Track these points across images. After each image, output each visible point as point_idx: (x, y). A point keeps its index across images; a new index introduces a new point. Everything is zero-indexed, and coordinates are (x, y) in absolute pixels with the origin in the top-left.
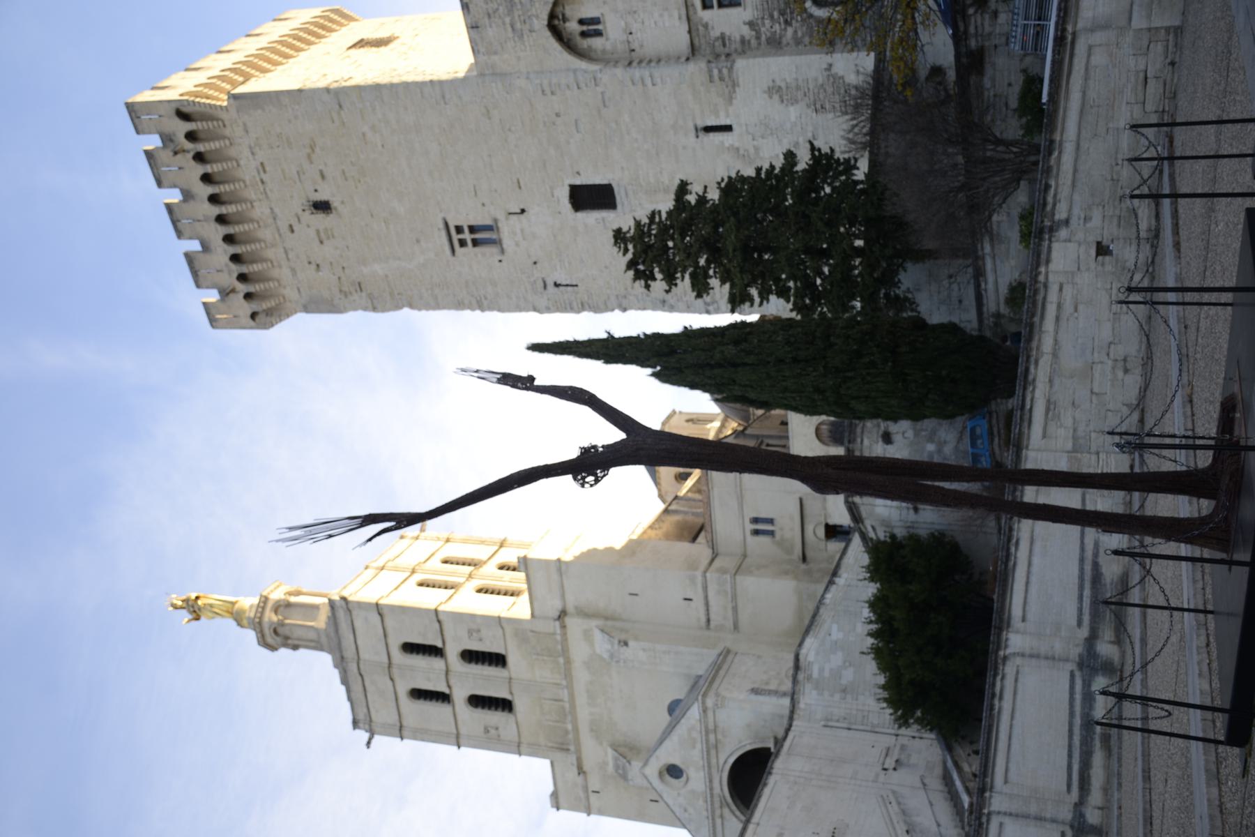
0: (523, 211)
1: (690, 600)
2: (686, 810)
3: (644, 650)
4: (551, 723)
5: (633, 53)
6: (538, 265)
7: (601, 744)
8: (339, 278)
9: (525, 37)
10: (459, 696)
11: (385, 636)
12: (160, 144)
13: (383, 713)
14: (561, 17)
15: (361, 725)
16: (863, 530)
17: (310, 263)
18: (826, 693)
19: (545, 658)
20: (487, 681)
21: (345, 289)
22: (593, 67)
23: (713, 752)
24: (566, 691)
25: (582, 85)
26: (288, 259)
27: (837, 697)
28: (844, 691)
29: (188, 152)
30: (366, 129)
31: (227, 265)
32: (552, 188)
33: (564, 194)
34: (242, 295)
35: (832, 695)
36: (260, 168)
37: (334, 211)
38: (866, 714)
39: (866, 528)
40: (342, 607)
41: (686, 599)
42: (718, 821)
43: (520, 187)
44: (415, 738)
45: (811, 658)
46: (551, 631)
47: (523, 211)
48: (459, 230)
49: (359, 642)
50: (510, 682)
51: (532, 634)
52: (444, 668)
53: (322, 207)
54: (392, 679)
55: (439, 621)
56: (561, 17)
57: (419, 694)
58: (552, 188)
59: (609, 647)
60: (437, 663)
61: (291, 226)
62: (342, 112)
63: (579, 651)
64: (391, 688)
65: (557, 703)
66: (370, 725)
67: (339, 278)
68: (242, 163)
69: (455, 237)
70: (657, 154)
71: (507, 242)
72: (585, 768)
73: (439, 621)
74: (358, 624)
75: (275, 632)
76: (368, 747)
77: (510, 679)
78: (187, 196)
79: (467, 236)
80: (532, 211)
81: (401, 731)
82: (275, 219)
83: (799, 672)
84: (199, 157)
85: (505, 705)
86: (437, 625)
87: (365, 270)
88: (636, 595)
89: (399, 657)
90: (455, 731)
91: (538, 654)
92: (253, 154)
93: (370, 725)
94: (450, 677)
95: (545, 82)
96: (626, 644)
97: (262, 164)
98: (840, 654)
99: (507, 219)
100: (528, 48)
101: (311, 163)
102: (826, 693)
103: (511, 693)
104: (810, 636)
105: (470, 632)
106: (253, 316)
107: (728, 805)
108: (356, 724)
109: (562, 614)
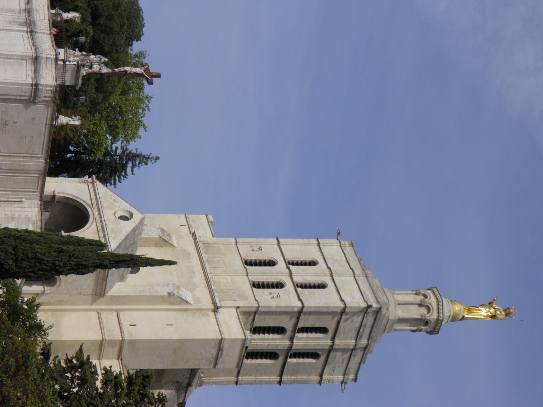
1: (131, 325)
2: (114, 200)
3: (157, 292)
4: (217, 256)
7: (182, 248)
10: (281, 265)
11: (338, 290)
18: (23, 216)
19: (225, 288)
23: (100, 228)
24: (208, 271)
27: (17, 215)
28: (13, 218)
35: (20, 215)
41: (135, 325)
42: (93, 197)
46: (222, 302)
49: (357, 286)
50: (247, 273)
51: (236, 299)
52: (294, 277)
54: (329, 268)
59: (181, 293)
60: (298, 279)
64: (328, 264)
65: (215, 266)
66: (340, 244)
72: (191, 235)
73: (300, 300)
74: (359, 295)
75: (425, 296)
77: (247, 276)
85: (249, 263)
86: (301, 298)
88: (167, 325)
89: (327, 280)
90: (282, 246)
91: (230, 289)
93: (340, 244)
96: (169, 294)
102: (23, 216)
103: (246, 268)
105: (278, 296)
107: (88, 205)
109: (216, 309)
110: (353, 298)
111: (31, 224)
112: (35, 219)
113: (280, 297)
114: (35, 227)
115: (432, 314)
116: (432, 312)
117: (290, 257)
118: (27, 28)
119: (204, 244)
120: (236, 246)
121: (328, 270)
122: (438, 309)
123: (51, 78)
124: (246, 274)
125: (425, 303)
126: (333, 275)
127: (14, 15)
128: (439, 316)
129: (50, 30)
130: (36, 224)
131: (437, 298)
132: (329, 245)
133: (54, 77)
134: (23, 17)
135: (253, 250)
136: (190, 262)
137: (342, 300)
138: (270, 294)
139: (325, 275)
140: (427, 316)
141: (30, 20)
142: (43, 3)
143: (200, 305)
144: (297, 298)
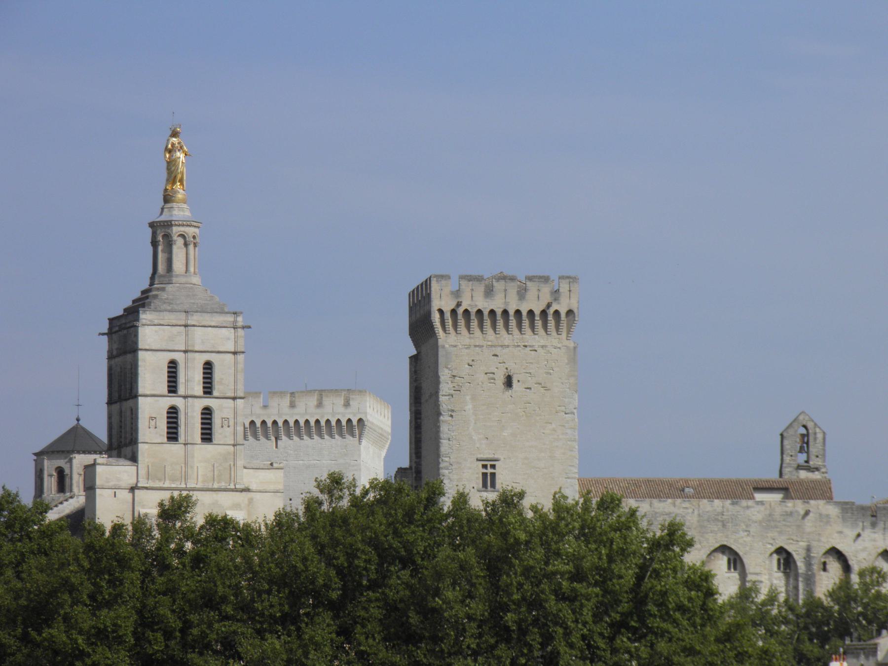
11: (219, 352)
20: (191, 425)
26: (475, 346)
30: (554, 426)
36: (533, 349)
48: (493, 467)
49: (210, 328)
53: (509, 382)
60: (199, 390)
62: (563, 413)
69: (489, 463)
79: (490, 470)
82: (502, 346)
84: (544, 313)
87: (468, 398)
92: (542, 347)
97: (536, 351)
109: (247, 490)
110: (229, 339)
138: (222, 427)
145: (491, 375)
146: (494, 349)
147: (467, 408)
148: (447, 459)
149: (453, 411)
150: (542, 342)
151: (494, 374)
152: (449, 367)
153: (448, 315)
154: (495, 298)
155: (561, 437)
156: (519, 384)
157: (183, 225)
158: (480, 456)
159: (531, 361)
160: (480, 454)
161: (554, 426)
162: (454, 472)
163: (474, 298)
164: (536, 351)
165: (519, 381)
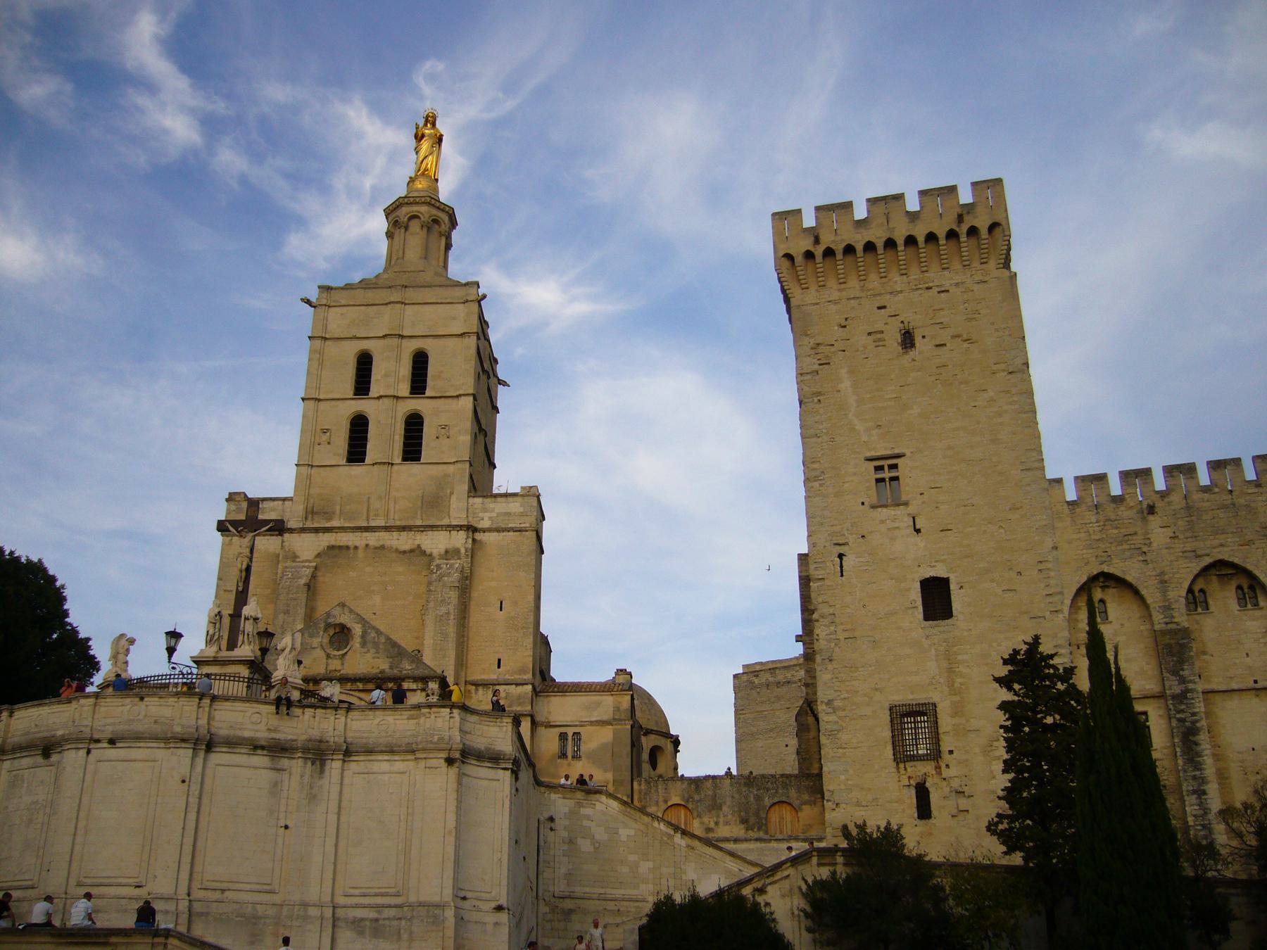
0: (918, 531)
5: (1076, 647)
6: (861, 540)
7: (318, 555)
8: (833, 345)
9: (1091, 551)
12: (962, 201)
13: (337, 321)
14: (1107, 584)
15: (325, 295)
16: (784, 867)
17: (846, 319)
18: (567, 822)
21: (821, 349)
22: (1066, 609)
25: (1050, 599)
27: (565, 834)
29: (958, 226)
30: (990, 393)
31: (842, 240)
32: (943, 561)
33: (940, 572)
34: (811, 248)
36: (943, 289)
37: (904, 350)
38: (552, 864)
39: (787, 869)
40: (467, 295)
43: (942, 531)
44: (312, 352)
45: (599, 806)
47: (918, 531)
52: (400, 394)
53: (908, 340)
54: (385, 336)
55: (458, 396)
56: (1107, 584)
57: (364, 364)
58: (943, 561)
60: (404, 389)
61: (884, 307)
62: (1005, 373)
63: (435, 543)
66: (326, 305)
67: (833, 345)
68: (946, 272)
69: (886, 463)
70: (987, 664)
71: (884, 513)
73: (458, 396)
76: (301, 299)
78: (913, 216)
80: (918, 539)
81: (319, 338)
82: (891, 293)
83: (583, 793)
84: (952, 235)
87: (843, 372)
89: (411, 347)
92: (957, 284)
94: (392, 399)
95: (1050, 565)
97: (948, 291)
98: (605, 837)
99: (909, 515)
100: (1082, 552)
101: (954, 337)
104: (620, 805)
106: (789, 257)
108: (326, 289)
109: (472, 529)
110: (454, 318)
111: (581, 809)
112: (572, 801)
113: (446, 426)
114: (586, 803)
115: (443, 221)
116: (441, 219)
117: (348, 387)
118: (332, 760)
119: (306, 518)
120: (314, 468)
121: (388, 341)
122: (438, 208)
123: (491, 728)
124: (390, 466)
125: (428, 223)
126: (401, 333)
127: (286, 783)
128: (447, 212)
129: (336, 711)
130: (581, 801)
131: (423, 203)
132: (326, 324)
133: (488, 719)
134: (296, 767)
135: (329, 443)
136: (356, 548)
137: (462, 335)
139: (399, 347)
140: (443, 226)
141: (306, 750)
142: (248, 714)
143: (463, 551)
144: (450, 401)
145: (879, 336)
146: (878, 298)
147: (842, 386)
148: (816, 466)
149: (819, 394)
150: (957, 279)
151: (882, 332)
152: (809, 333)
153: (799, 260)
154: (872, 226)
155: (1005, 408)
156: (925, 340)
157: (417, 203)
158: (869, 454)
159: (940, 307)
160: (870, 450)
161: (990, 393)
162: (828, 483)
163: (837, 231)
164: (948, 291)
165: (924, 337)
